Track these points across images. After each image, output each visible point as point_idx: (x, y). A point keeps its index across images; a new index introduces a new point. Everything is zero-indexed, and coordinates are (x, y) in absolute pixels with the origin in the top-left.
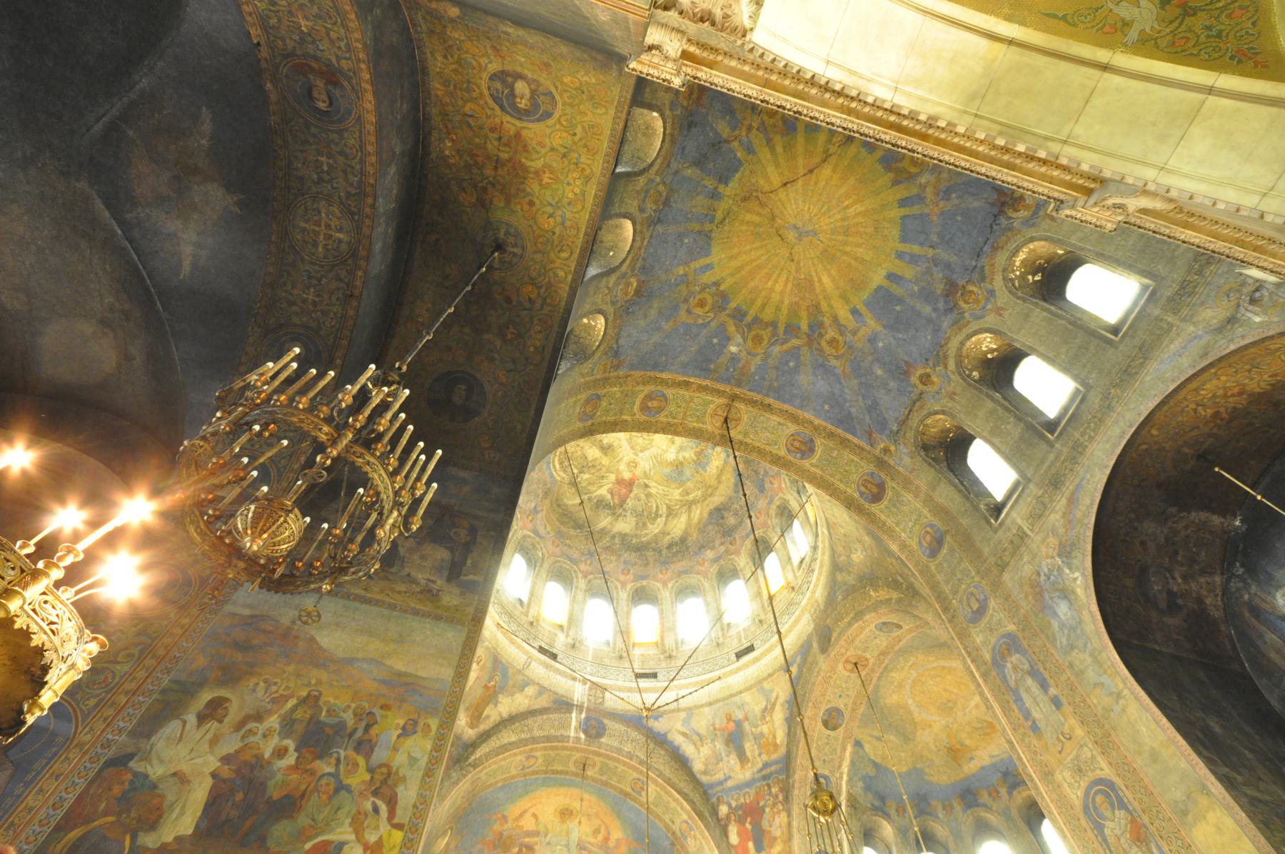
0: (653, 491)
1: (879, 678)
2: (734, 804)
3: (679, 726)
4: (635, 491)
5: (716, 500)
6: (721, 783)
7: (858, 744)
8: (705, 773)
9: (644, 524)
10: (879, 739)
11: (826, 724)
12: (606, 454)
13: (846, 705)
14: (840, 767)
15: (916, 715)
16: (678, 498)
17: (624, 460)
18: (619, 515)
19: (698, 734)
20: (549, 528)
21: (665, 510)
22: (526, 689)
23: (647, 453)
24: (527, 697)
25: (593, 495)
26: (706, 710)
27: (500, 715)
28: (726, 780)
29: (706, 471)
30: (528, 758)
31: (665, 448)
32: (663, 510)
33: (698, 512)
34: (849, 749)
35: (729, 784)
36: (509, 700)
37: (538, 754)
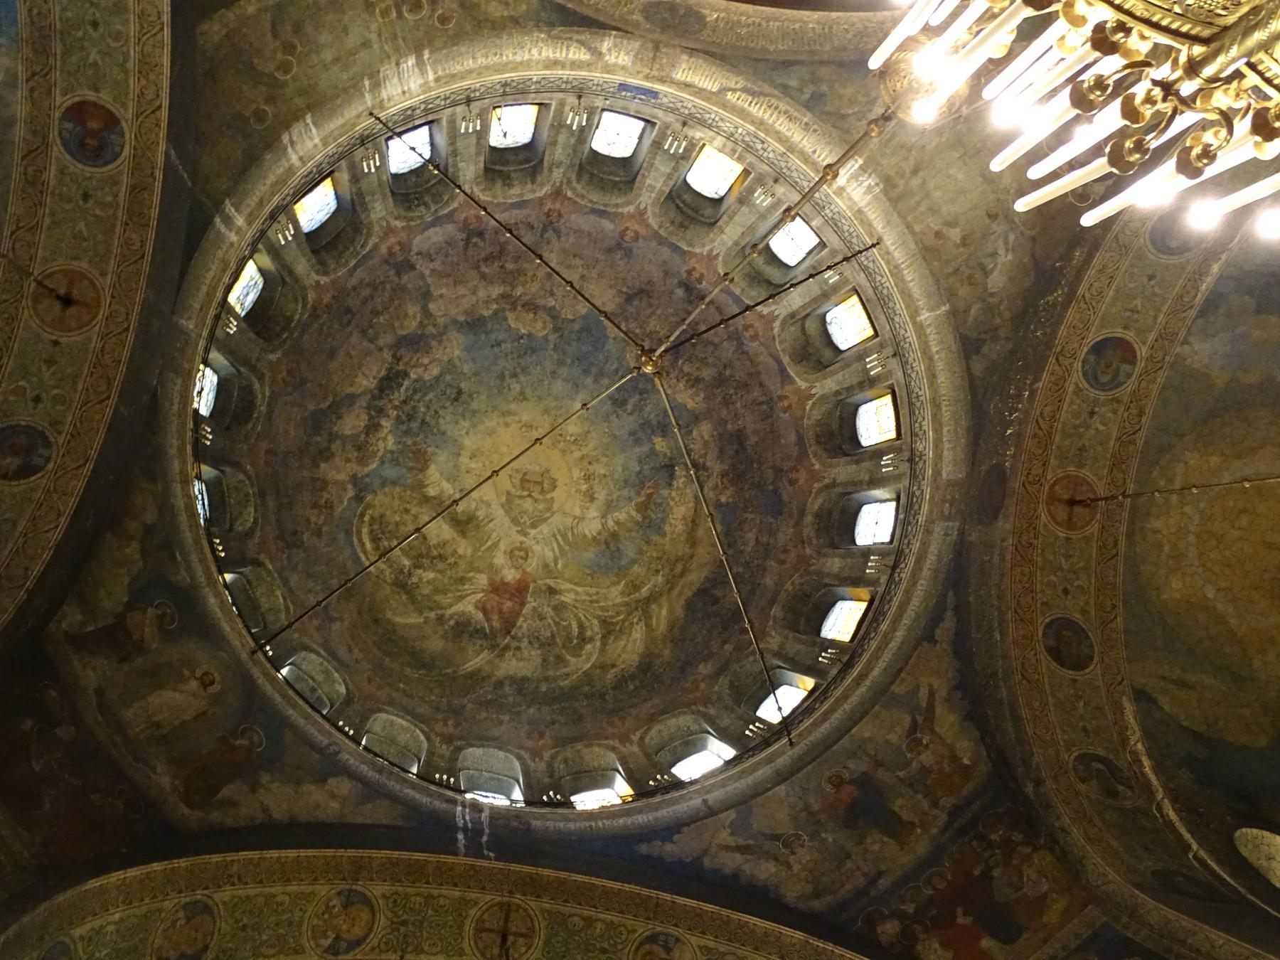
0: (567, 598)
1: (1130, 535)
2: (910, 908)
3: (725, 837)
4: (531, 603)
5: (696, 577)
6: (861, 893)
7: (1141, 696)
8: (817, 894)
9: (560, 660)
10: (1183, 684)
11: (1057, 654)
12: (463, 534)
13: (1084, 612)
14: (1125, 741)
15: (1233, 622)
16: (619, 600)
17: (502, 546)
18: (507, 648)
19: (776, 837)
20: (357, 654)
21: (596, 629)
22: (332, 782)
23: (544, 528)
24: (333, 796)
25: (449, 612)
26: (781, 790)
27: (265, 810)
28: (873, 881)
29: (664, 535)
30: (350, 900)
31: (577, 512)
32: (595, 627)
33: (664, 612)
34: (1129, 710)
35: (883, 883)
36: (289, 790)
37: (377, 890)
